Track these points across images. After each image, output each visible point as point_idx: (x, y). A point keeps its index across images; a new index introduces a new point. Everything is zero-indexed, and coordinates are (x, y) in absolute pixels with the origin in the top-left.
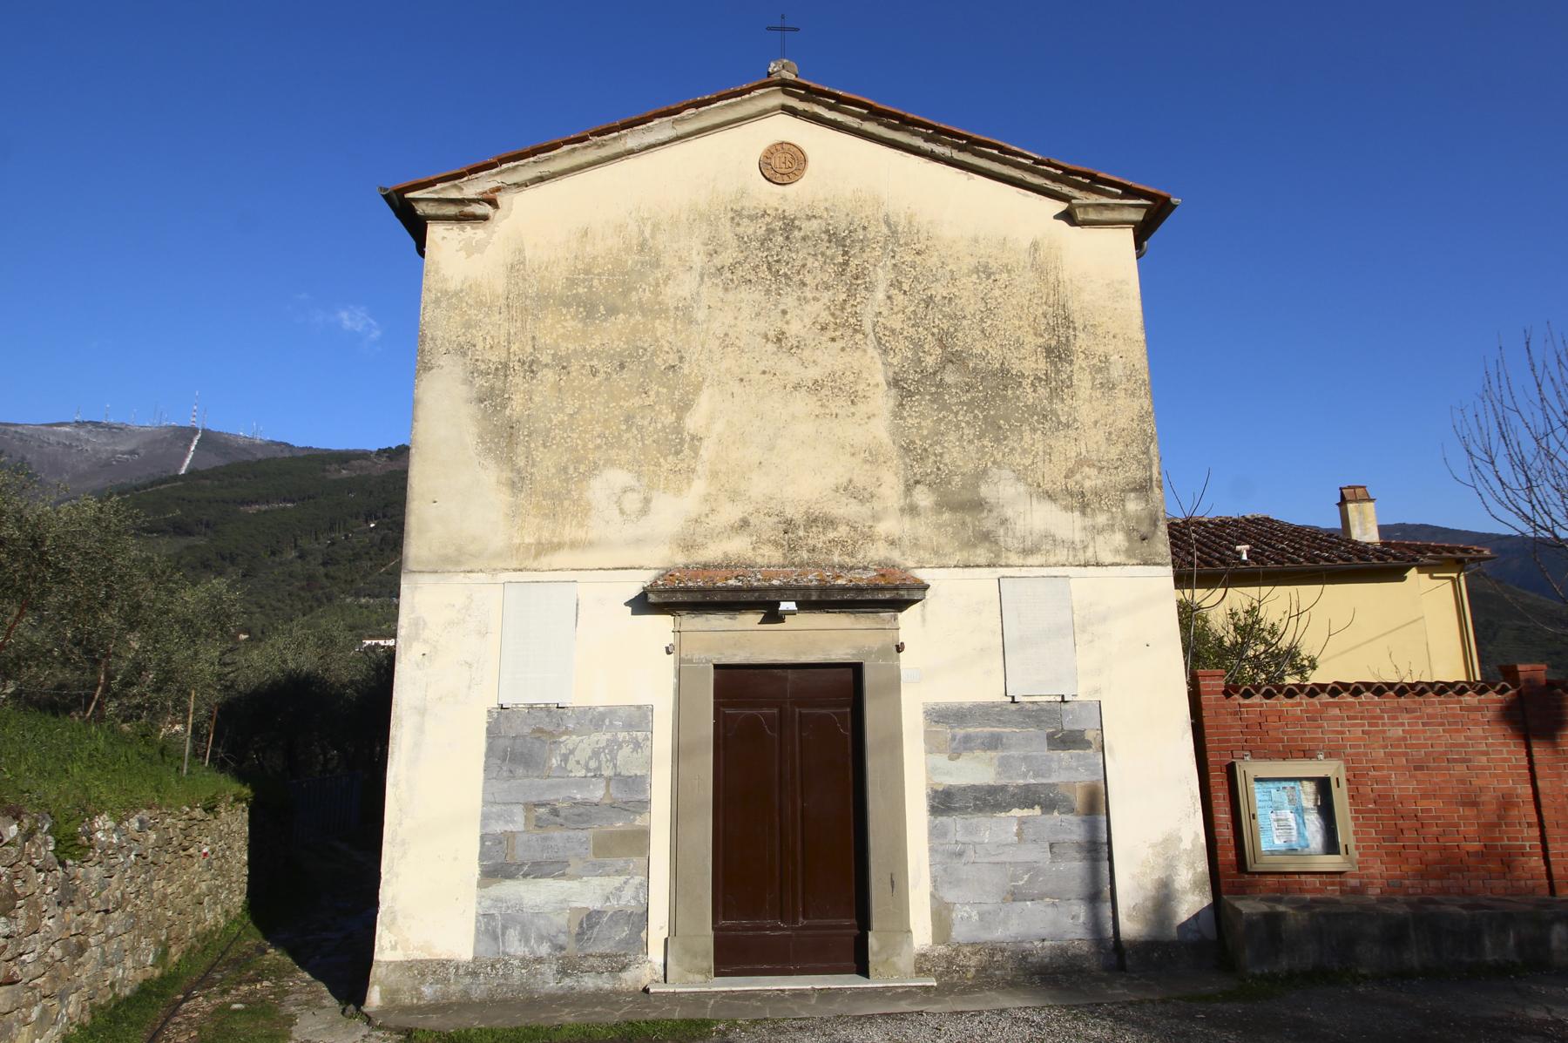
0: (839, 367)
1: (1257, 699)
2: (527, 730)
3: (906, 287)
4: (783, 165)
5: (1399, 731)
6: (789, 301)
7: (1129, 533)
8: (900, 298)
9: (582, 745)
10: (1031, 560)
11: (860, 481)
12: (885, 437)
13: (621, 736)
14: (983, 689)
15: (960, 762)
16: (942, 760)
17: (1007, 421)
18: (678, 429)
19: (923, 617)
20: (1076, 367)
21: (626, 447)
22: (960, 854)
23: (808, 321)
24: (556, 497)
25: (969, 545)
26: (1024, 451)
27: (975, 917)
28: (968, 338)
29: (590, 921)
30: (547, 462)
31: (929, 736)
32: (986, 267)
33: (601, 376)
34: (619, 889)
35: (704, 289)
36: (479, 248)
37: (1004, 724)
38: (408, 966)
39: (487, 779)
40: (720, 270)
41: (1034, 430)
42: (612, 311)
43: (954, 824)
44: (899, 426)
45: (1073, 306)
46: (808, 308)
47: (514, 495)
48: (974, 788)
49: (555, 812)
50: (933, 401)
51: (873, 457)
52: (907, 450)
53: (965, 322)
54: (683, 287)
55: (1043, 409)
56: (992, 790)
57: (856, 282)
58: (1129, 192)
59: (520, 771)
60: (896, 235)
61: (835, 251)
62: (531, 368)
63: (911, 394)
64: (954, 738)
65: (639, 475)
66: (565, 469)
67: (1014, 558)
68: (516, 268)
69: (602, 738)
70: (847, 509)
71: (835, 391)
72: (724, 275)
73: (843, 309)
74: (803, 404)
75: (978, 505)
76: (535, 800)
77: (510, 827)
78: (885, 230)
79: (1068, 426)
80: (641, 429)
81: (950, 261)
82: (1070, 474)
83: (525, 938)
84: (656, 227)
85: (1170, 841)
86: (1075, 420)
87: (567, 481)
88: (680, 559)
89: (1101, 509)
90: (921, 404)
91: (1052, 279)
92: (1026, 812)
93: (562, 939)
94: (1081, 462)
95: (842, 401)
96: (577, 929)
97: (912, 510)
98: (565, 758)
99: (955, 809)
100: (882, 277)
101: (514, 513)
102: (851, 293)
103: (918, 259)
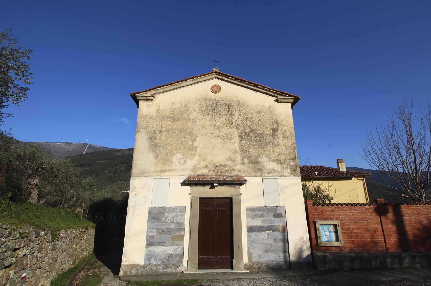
0: (227, 132)
1: (320, 206)
2: (157, 212)
3: (242, 115)
4: (216, 89)
6: (217, 118)
7: (291, 169)
8: (241, 118)
9: (170, 215)
10: (269, 175)
11: (232, 157)
12: (238, 148)
13: (178, 213)
15: (254, 220)
16: (250, 220)
18: (192, 145)
19: (246, 188)
21: (181, 149)
22: (254, 241)
23: (221, 122)
25: (256, 171)
26: (268, 151)
27: (258, 256)
28: (255, 126)
29: (171, 255)
30: (164, 153)
32: (259, 111)
33: (176, 134)
34: (177, 249)
35: (198, 115)
37: (264, 212)
38: (129, 266)
39: (148, 223)
40: (202, 111)
41: (270, 146)
42: (179, 120)
43: (253, 234)
44: (240, 145)
45: (278, 120)
46: (221, 119)
47: (156, 159)
48: (257, 226)
49: (163, 231)
51: (235, 152)
52: (242, 150)
54: (194, 115)
56: (261, 227)
57: (232, 114)
58: (290, 96)
59: (156, 221)
62: (161, 132)
63: (243, 138)
64: (253, 215)
65: (184, 155)
66: (168, 154)
67: (266, 174)
68: (158, 110)
69: (174, 214)
70: (229, 163)
73: (228, 120)
74: (219, 140)
75: (258, 163)
76: (159, 228)
77: (153, 234)
78: (237, 103)
80: (184, 145)
82: (278, 156)
84: (188, 102)
85: (302, 239)
87: (168, 156)
88: (192, 174)
90: (245, 140)
91: (273, 114)
92: (269, 232)
93: (164, 260)
94: (280, 153)
96: (167, 258)
97: (243, 163)
98: (166, 218)
99: (253, 231)
100: (237, 113)
101: (156, 163)
102: (230, 117)
103: (245, 109)
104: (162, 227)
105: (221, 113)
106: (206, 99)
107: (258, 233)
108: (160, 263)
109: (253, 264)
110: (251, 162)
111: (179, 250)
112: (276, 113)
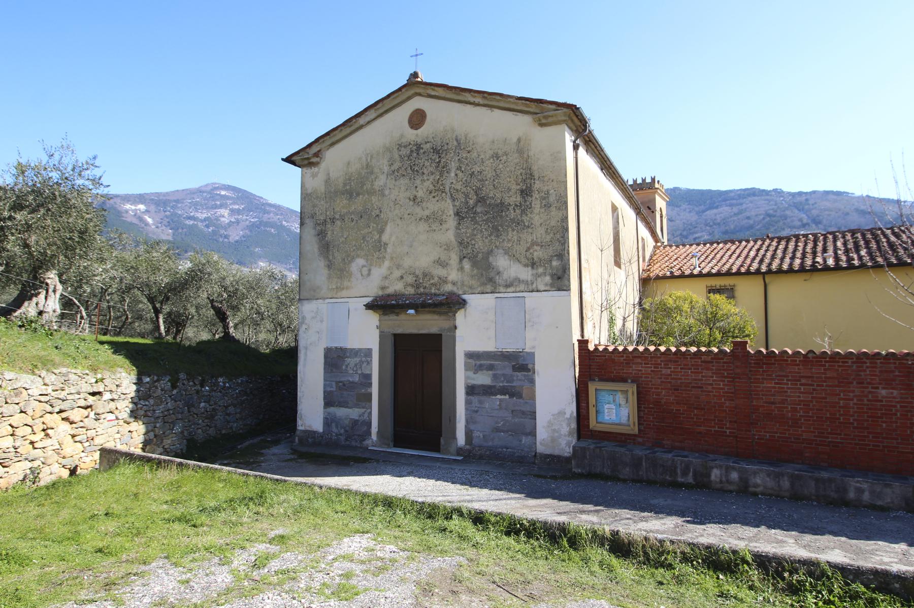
0: (436, 209)
5: (669, 371)
6: (418, 182)
7: (552, 276)
8: (460, 175)
9: (352, 361)
10: (509, 290)
11: (443, 258)
12: (453, 239)
13: (363, 359)
14: (487, 345)
16: (471, 374)
18: (380, 241)
21: (363, 249)
22: (477, 412)
24: (342, 270)
26: (509, 240)
28: (488, 190)
29: (355, 423)
30: (339, 256)
31: (466, 364)
32: (497, 154)
36: (314, 176)
37: (496, 360)
38: (305, 431)
39: (325, 372)
41: (513, 230)
42: (358, 194)
43: (475, 399)
45: (535, 168)
49: (344, 385)
51: (448, 248)
52: (461, 243)
54: (381, 181)
56: (490, 387)
57: (442, 169)
60: (461, 145)
61: (436, 157)
62: (333, 220)
63: (463, 218)
65: (367, 260)
67: (502, 289)
68: (327, 181)
69: (357, 360)
71: (434, 219)
72: (395, 174)
74: (423, 226)
78: (455, 143)
79: (528, 227)
82: (528, 249)
83: (337, 427)
84: (372, 157)
85: (562, 413)
87: (345, 264)
88: (380, 293)
90: (467, 222)
91: (525, 156)
92: (503, 397)
94: (534, 243)
95: (437, 224)
98: (347, 366)
101: (329, 277)
102: (441, 176)
104: (342, 379)
105: (425, 171)
106: (400, 145)
107: (483, 398)
108: (342, 431)
109: (473, 448)
110: (475, 264)
111: (366, 415)
112: (531, 153)
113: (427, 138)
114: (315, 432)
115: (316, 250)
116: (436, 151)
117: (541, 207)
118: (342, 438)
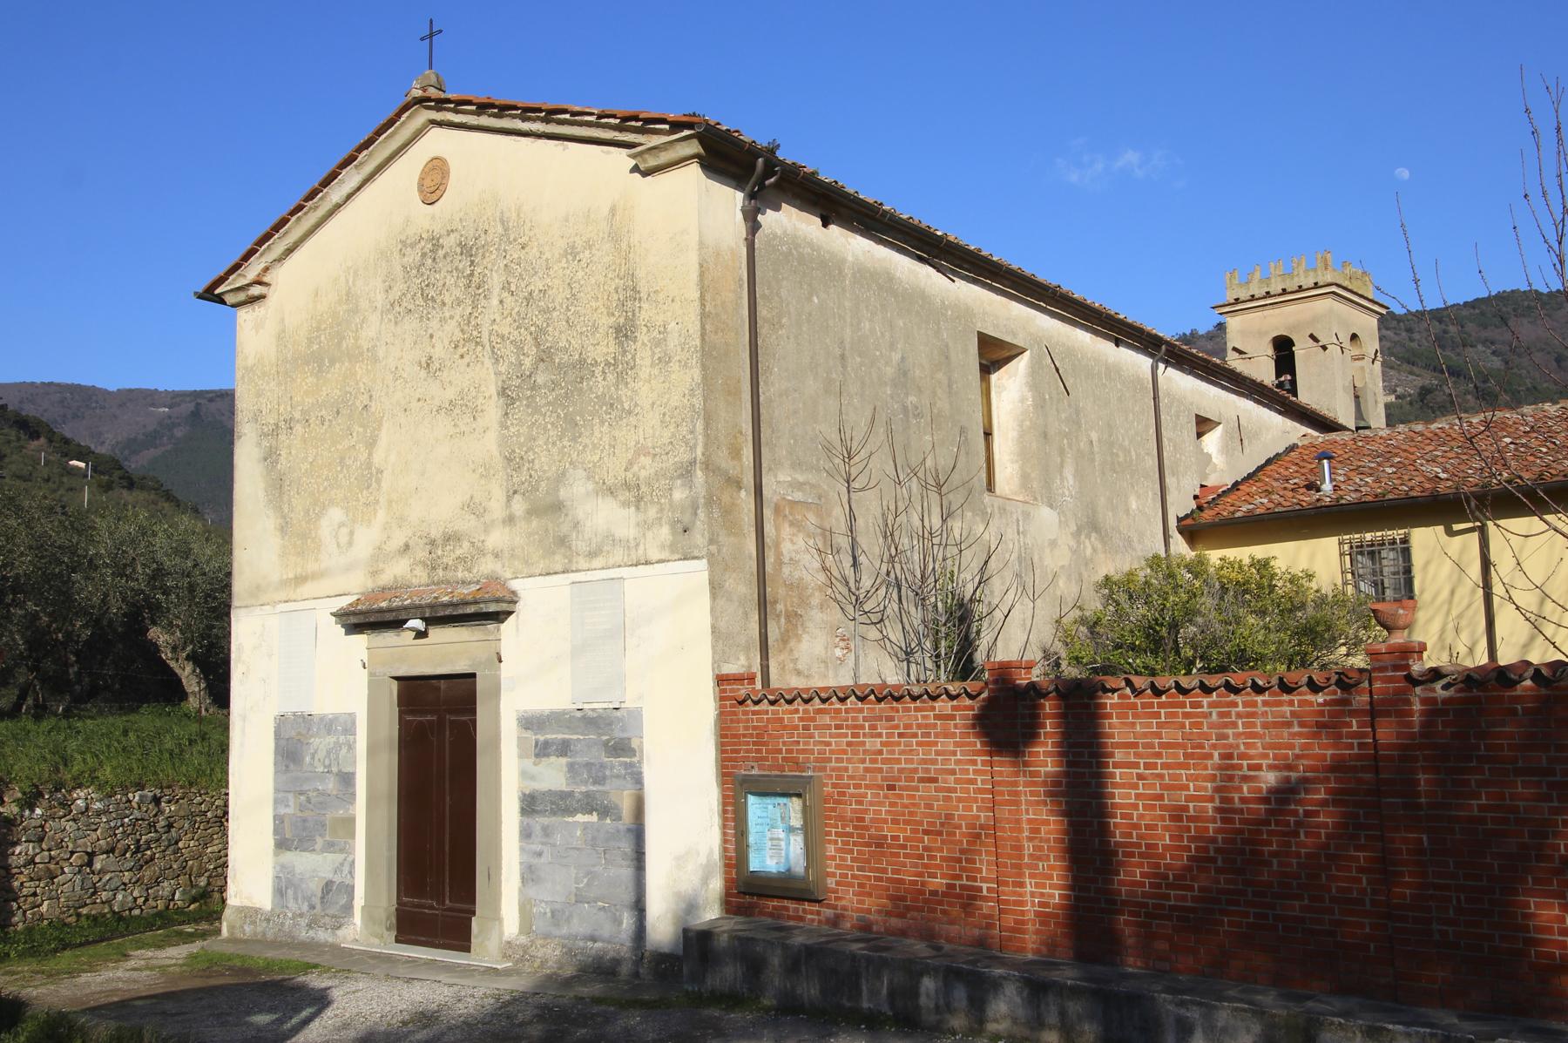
1: (764, 706)
4: (434, 183)
6: (434, 324)
8: (509, 300)
12: (496, 453)
13: (342, 739)
17: (582, 416)
20: (639, 344)
23: (446, 342)
25: (549, 553)
26: (595, 446)
28: (559, 335)
31: (521, 741)
32: (573, 247)
41: (602, 422)
42: (332, 362)
50: (528, 406)
52: (509, 460)
53: (555, 314)
55: (611, 397)
56: (564, 796)
58: (676, 126)
59: (292, 766)
62: (290, 423)
63: (513, 401)
67: (583, 564)
68: (281, 337)
69: (331, 739)
70: (466, 524)
71: (461, 407)
75: (557, 507)
78: (500, 230)
79: (630, 412)
80: (349, 467)
81: (546, 248)
82: (631, 463)
84: (356, 273)
86: (636, 405)
88: (370, 585)
89: (652, 502)
91: (624, 245)
94: (640, 451)
95: (468, 418)
97: (510, 520)
108: (305, 908)
111: (346, 869)
113: (451, 221)
114: (257, 911)
115: (261, 494)
116: (466, 250)
117: (652, 365)
118: (303, 922)
